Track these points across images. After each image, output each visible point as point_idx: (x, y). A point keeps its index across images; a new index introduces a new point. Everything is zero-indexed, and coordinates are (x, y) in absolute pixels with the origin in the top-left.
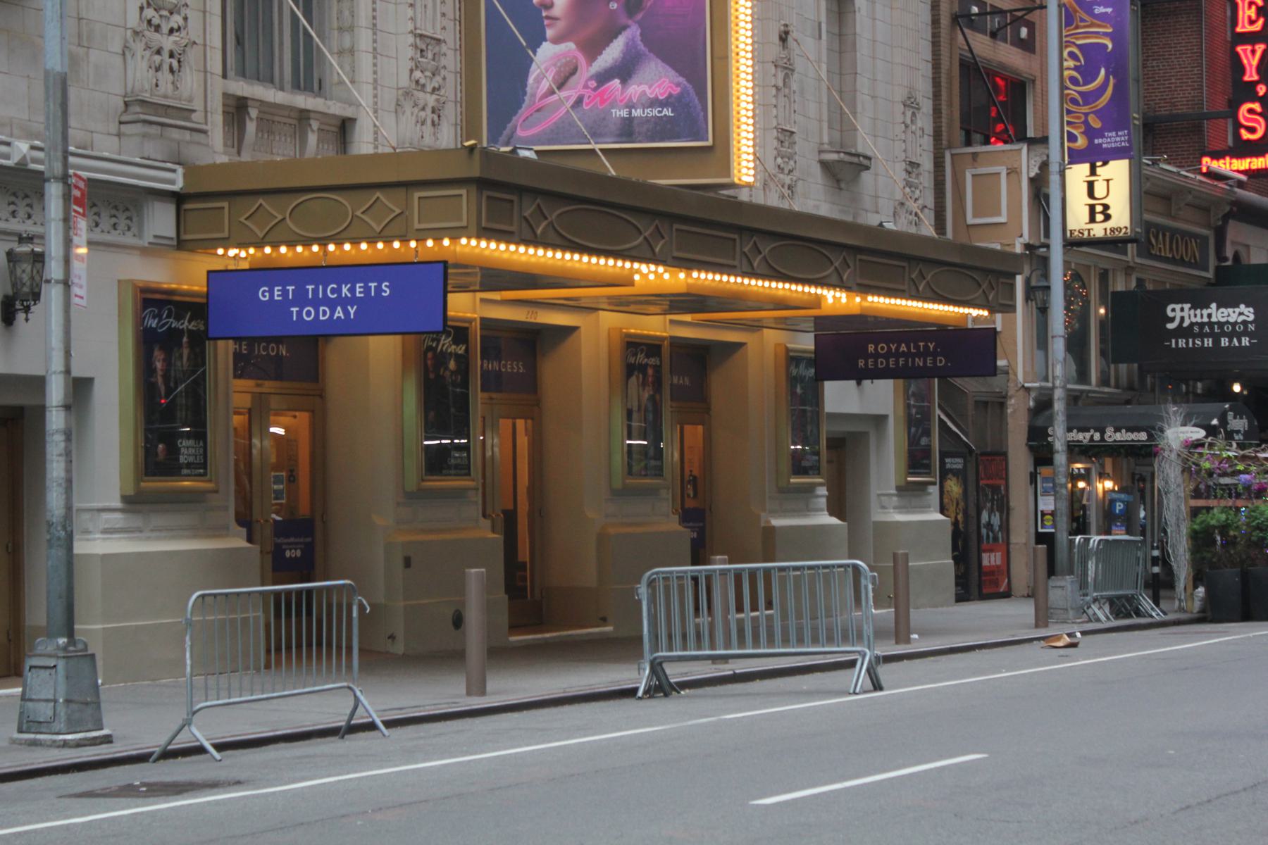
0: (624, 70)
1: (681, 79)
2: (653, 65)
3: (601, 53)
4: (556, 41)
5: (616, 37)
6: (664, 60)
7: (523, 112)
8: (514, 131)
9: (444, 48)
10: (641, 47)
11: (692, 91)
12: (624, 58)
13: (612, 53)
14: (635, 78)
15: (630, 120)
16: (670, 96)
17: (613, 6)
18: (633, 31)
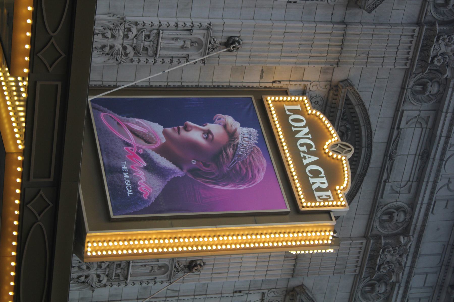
0: (152, 167)
1: (153, 199)
2: (160, 183)
3: (161, 155)
4: (165, 133)
5: (174, 164)
6: (164, 190)
7: (116, 116)
8: (102, 111)
9: (151, 60)
10: (170, 177)
11: (147, 205)
12: (161, 168)
13: (163, 162)
14: (148, 174)
15: (120, 171)
16: (142, 194)
17: (194, 162)
18: (179, 173)
